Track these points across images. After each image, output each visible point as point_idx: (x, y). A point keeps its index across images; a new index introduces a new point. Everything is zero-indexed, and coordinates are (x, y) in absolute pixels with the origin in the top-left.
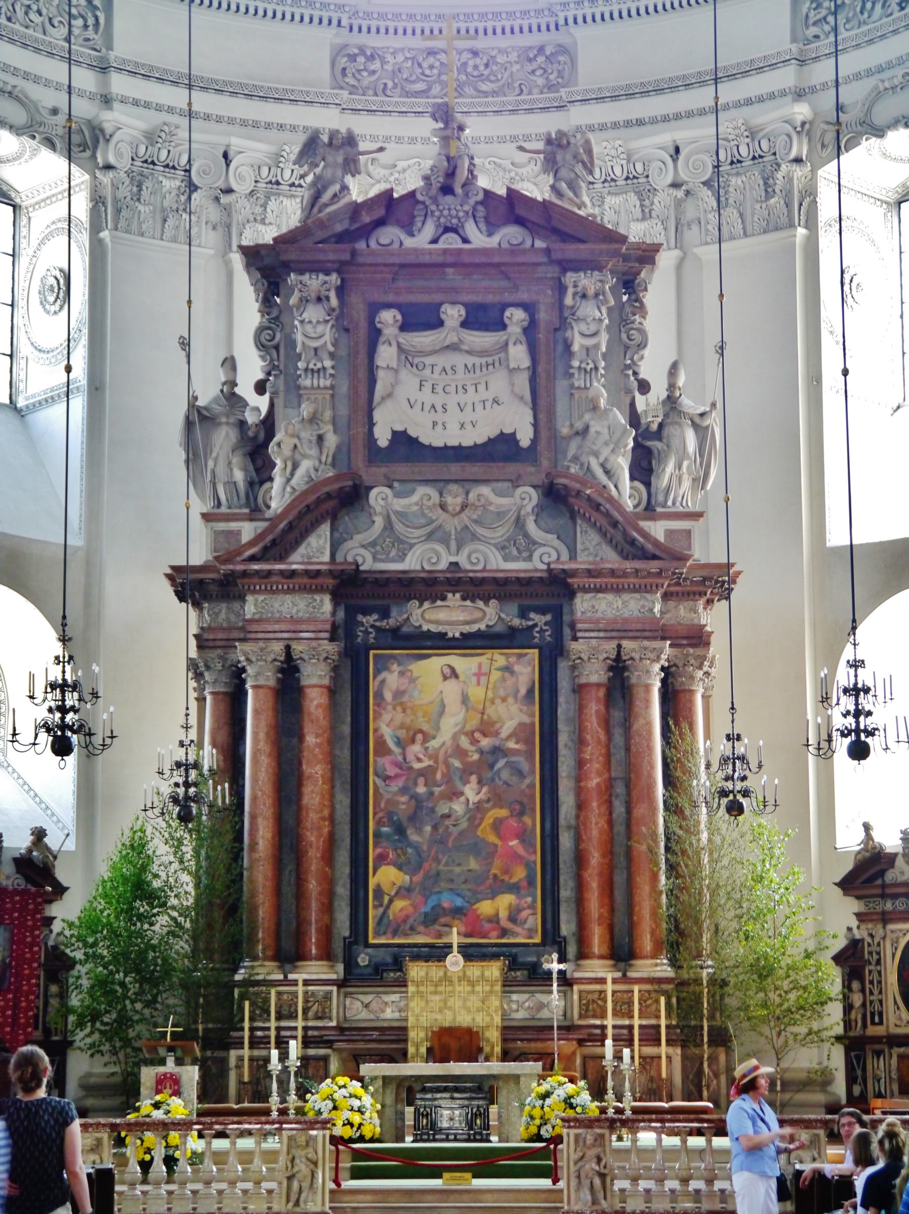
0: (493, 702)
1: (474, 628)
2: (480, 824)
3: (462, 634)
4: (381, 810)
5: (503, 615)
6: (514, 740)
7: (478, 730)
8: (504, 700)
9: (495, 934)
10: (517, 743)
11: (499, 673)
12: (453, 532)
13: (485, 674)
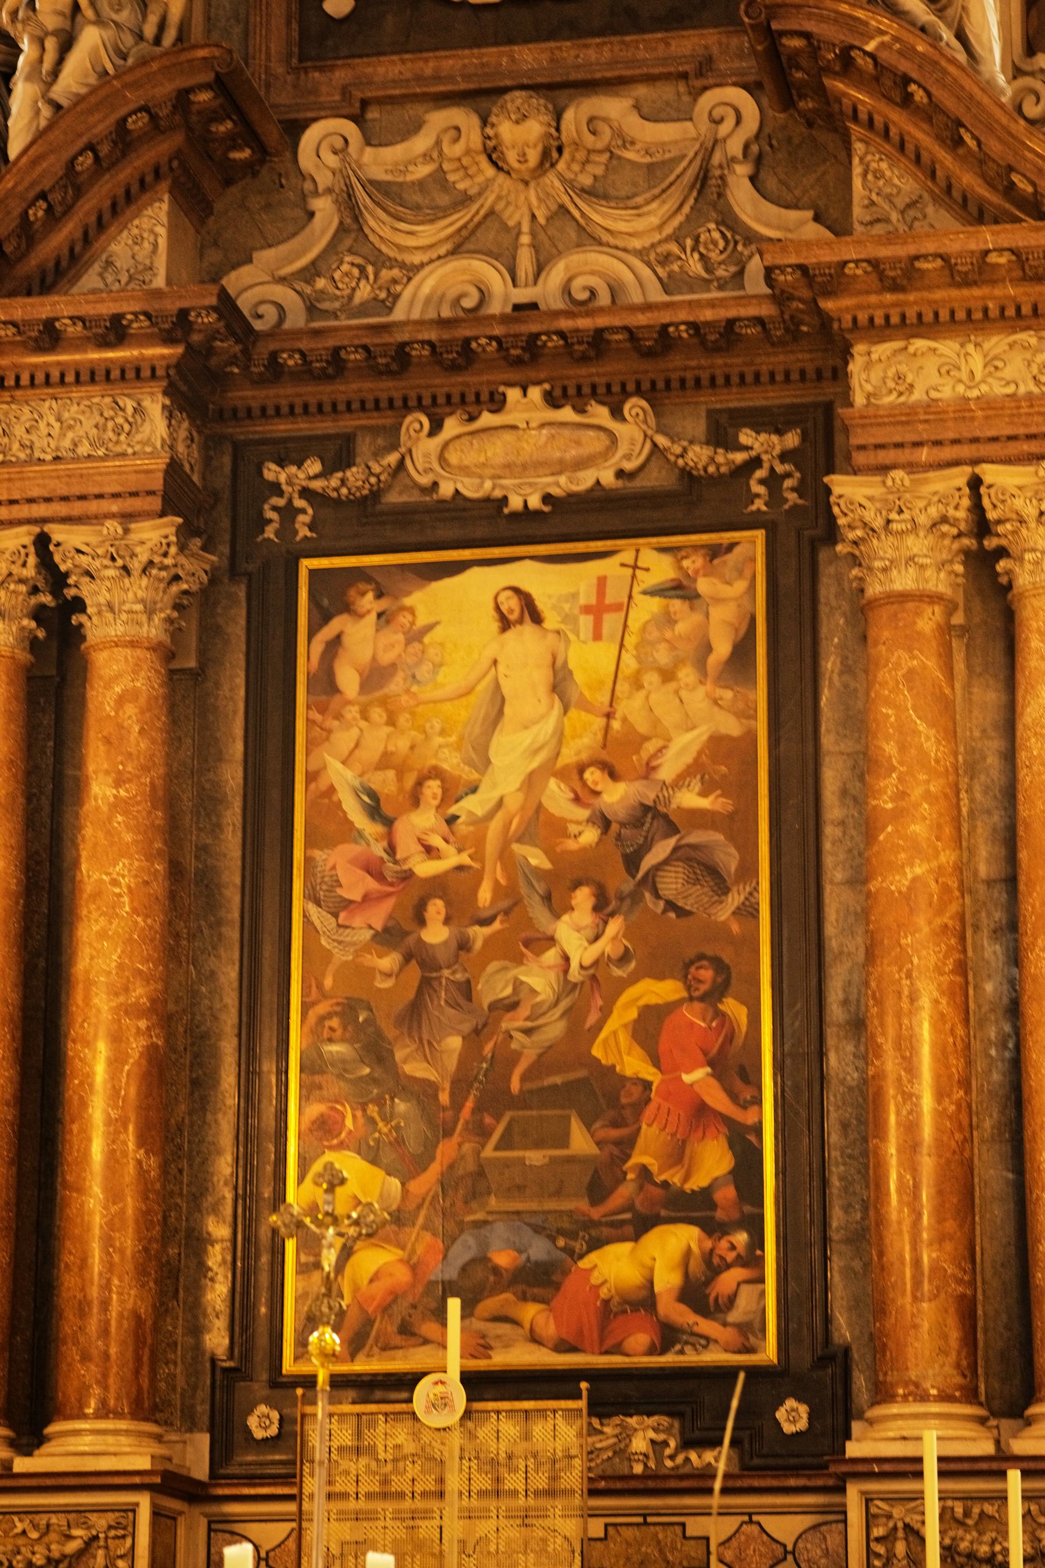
0: (637, 684)
1: (584, 481)
3: (547, 498)
4: (324, 995)
5: (662, 441)
6: (696, 785)
7: (593, 763)
9: (640, 1340)
10: (704, 794)
11: (655, 604)
12: (526, 227)
13: (616, 607)
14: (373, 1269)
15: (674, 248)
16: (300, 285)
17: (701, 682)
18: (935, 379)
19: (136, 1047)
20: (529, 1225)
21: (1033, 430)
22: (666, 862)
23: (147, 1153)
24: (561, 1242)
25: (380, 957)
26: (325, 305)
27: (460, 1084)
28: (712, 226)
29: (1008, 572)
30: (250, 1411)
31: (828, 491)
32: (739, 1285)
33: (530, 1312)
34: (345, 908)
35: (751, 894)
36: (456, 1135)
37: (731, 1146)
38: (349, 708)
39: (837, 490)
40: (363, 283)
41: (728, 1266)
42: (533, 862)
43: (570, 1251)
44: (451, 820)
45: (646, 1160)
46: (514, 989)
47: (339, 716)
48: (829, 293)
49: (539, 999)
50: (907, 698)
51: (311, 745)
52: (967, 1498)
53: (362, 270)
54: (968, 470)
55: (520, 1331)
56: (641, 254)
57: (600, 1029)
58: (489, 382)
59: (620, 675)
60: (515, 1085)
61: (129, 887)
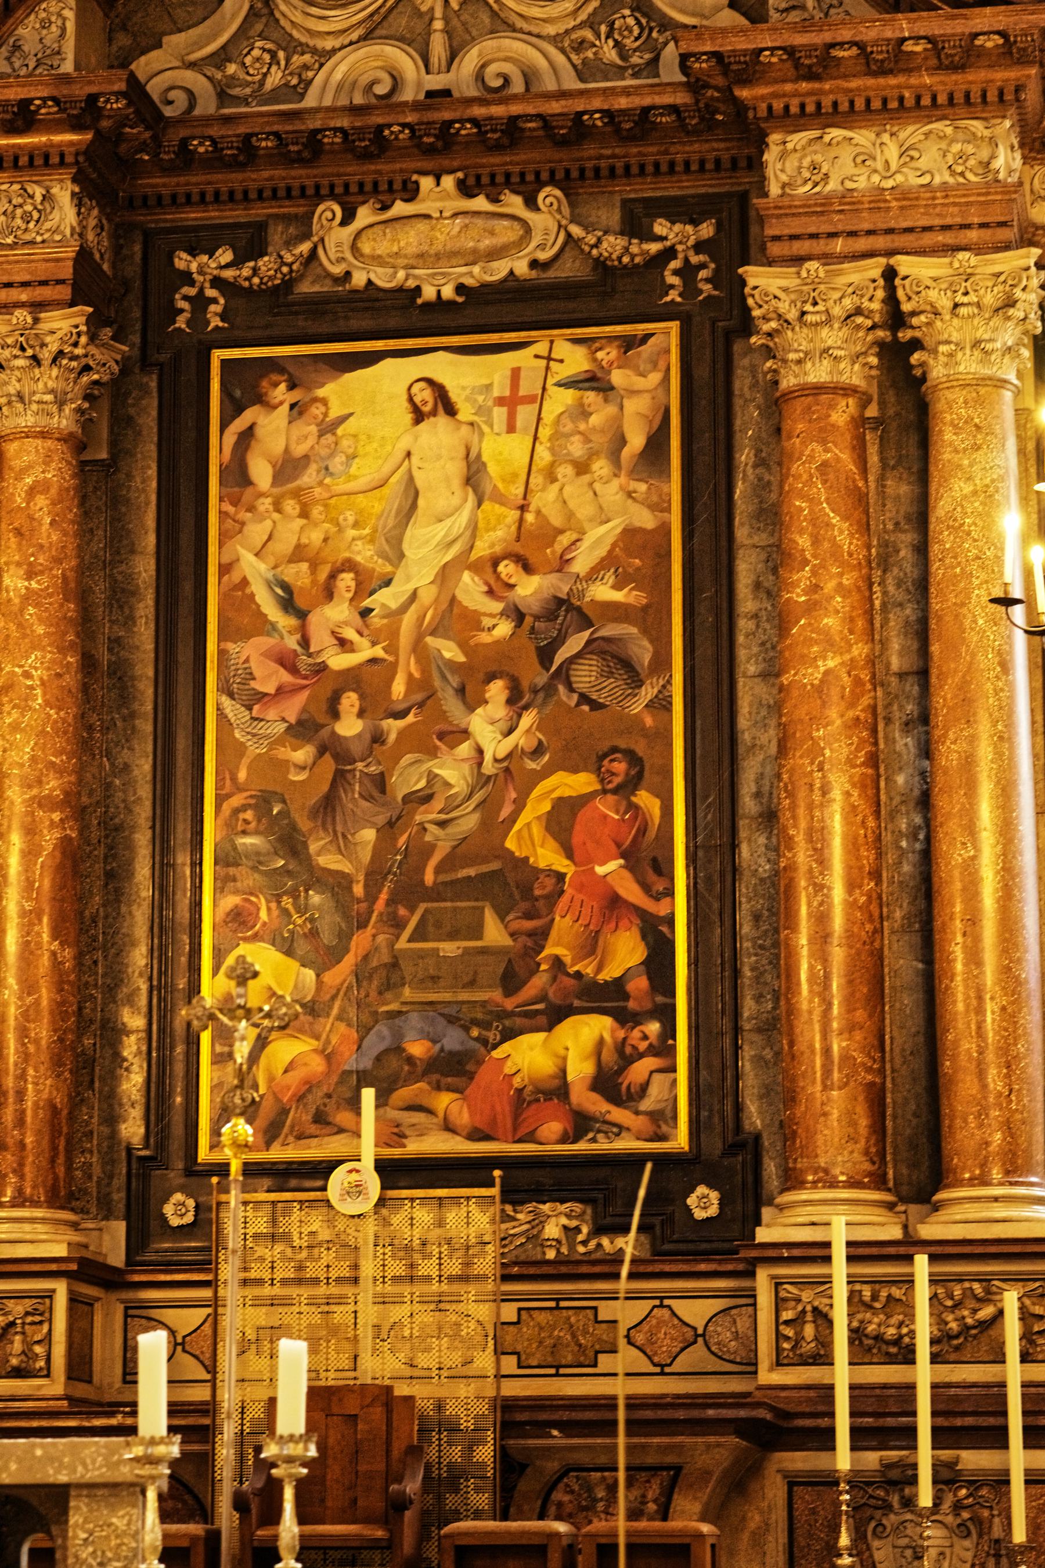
0: (551, 477)
1: (499, 270)
2: (513, 819)
3: (460, 289)
4: (239, 789)
5: (576, 230)
6: (610, 578)
7: (507, 556)
8: (582, 468)
9: (553, 1128)
10: (617, 587)
11: (569, 396)
12: (438, 13)
13: (530, 399)
14: (288, 1059)
15: (588, 34)
16: (210, 71)
17: (615, 475)
18: (850, 170)
19: (49, 839)
20: (442, 1015)
21: (949, 221)
22: (579, 655)
23: (61, 943)
24: (475, 1033)
25: (295, 750)
26: (236, 91)
27: (375, 876)
28: (627, 12)
29: (923, 364)
30: (166, 1200)
31: (743, 283)
32: (651, 1072)
33: (444, 1101)
34: (258, 701)
35: (664, 686)
36: (369, 928)
37: (644, 937)
38: (262, 500)
39: (751, 282)
40: (274, 68)
41: (641, 1056)
42: (447, 655)
43: (483, 1041)
44: (365, 613)
45: (559, 951)
46: (428, 782)
47: (251, 509)
48: (746, 81)
49: (452, 792)
50: (819, 489)
51: (224, 537)
52: (875, 1282)
53: (273, 55)
54: (883, 261)
55: (435, 1120)
56: (555, 40)
57: (514, 822)
58: (401, 171)
59: (534, 468)
60: (429, 878)
61: (41, 679)
